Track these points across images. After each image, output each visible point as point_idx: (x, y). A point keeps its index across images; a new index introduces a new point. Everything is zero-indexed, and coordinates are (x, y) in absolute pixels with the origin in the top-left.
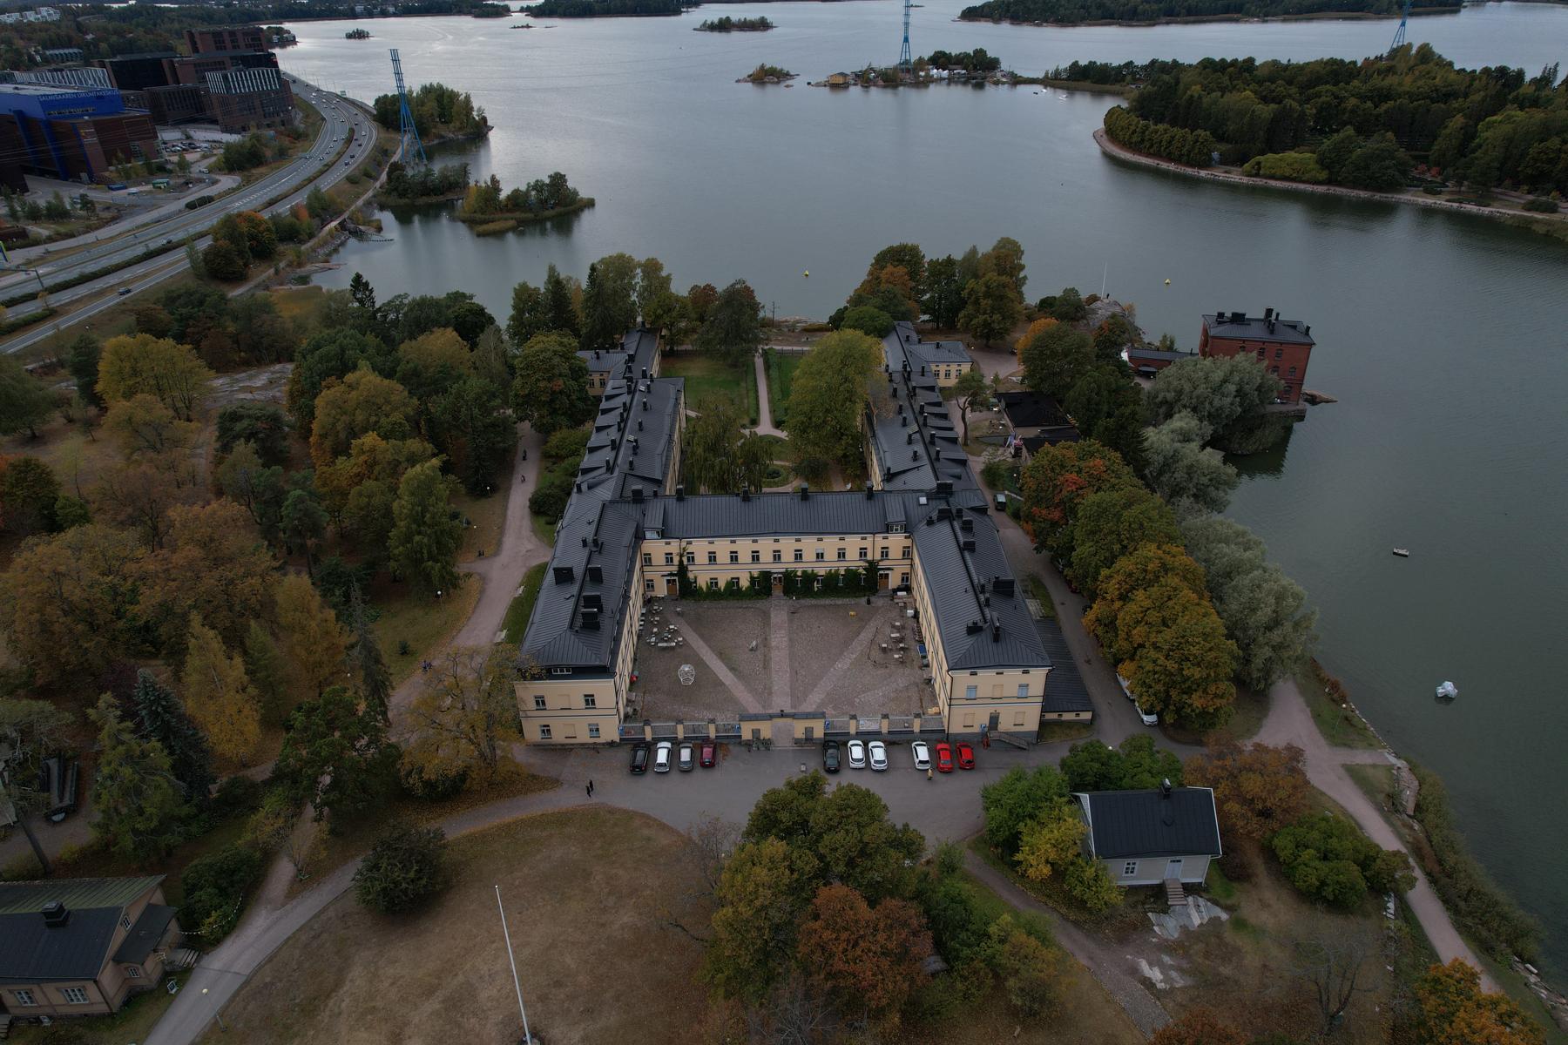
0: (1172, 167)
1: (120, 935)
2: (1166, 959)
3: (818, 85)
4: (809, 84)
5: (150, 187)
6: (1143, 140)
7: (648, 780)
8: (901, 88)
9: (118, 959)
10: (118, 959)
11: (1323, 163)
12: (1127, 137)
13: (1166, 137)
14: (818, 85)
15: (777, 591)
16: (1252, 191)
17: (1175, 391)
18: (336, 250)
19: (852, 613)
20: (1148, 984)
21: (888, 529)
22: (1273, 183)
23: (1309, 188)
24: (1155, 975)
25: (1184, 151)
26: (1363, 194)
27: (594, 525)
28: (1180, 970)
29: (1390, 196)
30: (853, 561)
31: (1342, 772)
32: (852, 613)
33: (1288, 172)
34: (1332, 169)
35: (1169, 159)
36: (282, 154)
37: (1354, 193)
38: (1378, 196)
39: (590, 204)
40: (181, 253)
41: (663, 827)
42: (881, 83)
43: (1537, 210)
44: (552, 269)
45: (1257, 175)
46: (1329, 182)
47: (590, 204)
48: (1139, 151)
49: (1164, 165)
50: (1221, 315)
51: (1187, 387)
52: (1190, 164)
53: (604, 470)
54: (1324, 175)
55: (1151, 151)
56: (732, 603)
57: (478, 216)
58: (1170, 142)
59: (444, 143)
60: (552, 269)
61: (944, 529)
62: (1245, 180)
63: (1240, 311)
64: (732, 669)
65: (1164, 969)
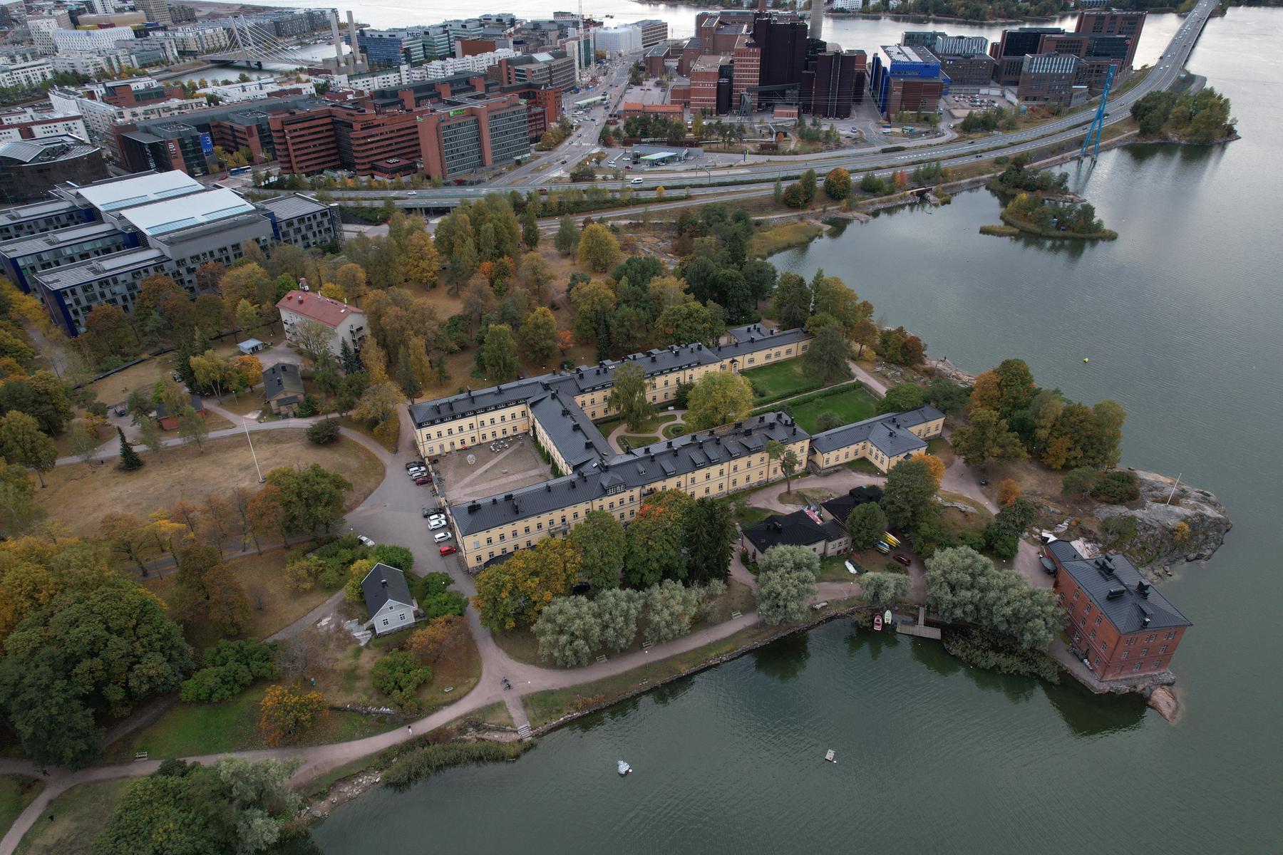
1: (282, 396)
2: (332, 626)
5: (898, 130)
7: (405, 472)
9: (278, 401)
10: (278, 401)
18: (890, 211)
20: (319, 621)
24: (324, 622)
28: (329, 629)
31: (496, 700)
36: (1011, 127)
40: (771, 185)
41: (379, 483)
47: (1112, 237)
57: (1009, 218)
59: (1164, 144)
60: (821, 271)
65: (328, 625)
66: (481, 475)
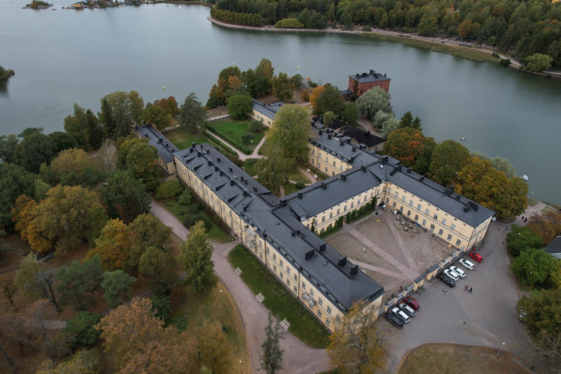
0: (250, 28)
3: (68, 8)
4: (63, 8)
6: (234, 19)
8: (108, 8)
11: (302, 21)
12: (227, 19)
13: (244, 17)
14: (68, 8)
15: (344, 224)
16: (279, 33)
17: (370, 104)
19: (378, 221)
21: (380, 181)
22: (288, 30)
23: (300, 30)
25: (253, 21)
26: (317, 30)
27: (281, 223)
29: (325, 30)
30: (369, 199)
32: (378, 221)
33: (291, 25)
34: (305, 23)
35: (247, 25)
37: (314, 30)
38: (321, 31)
39: (12, 73)
42: (98, 6)
43: (366, 31)
44: (76, 106)
45: (280, 27)
46: (305, 27)
48: (234, 24)
49: (247, 28)
50: (358, 75)
51: (375, 102)
52: (256, 26)
53: (241, 197)
54: (302, 25)
55: (239, 23)
56: (333, 235)
58: (246, 19)
61: (399, 174)
62: (278, 30)
63: (365, 72)
64: (369, 263)
66: (376, 265)
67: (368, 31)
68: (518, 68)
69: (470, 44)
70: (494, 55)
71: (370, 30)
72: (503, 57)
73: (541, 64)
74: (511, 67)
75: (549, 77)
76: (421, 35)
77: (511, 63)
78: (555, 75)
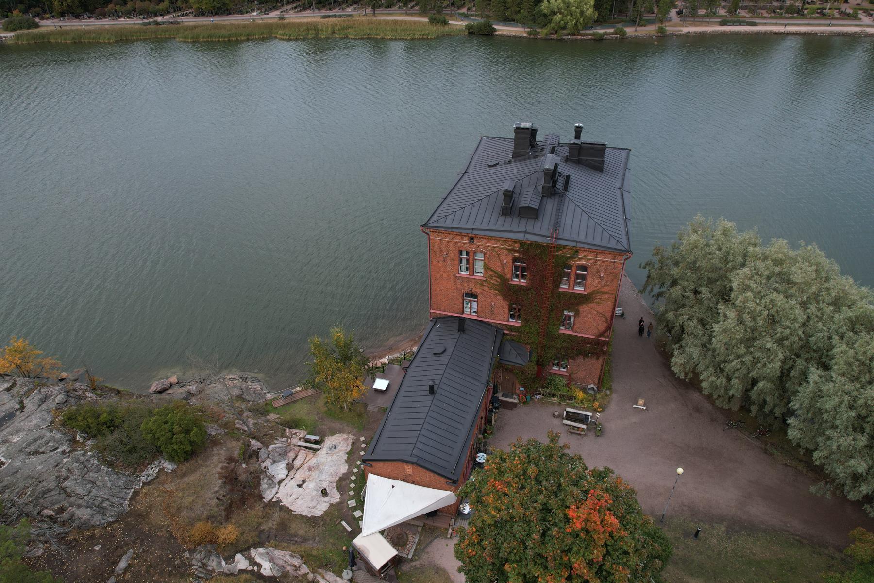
67: (29, 28)
68: (525, 35)
69: (336, 11)
70: (433, 21)
71: (37, 26)
72: (458, 24)
73: (582, 13)
74: (502, 36)
75: (600, 39)
76: (201, 13)
77: (495, 30)
78: (606, 34)
